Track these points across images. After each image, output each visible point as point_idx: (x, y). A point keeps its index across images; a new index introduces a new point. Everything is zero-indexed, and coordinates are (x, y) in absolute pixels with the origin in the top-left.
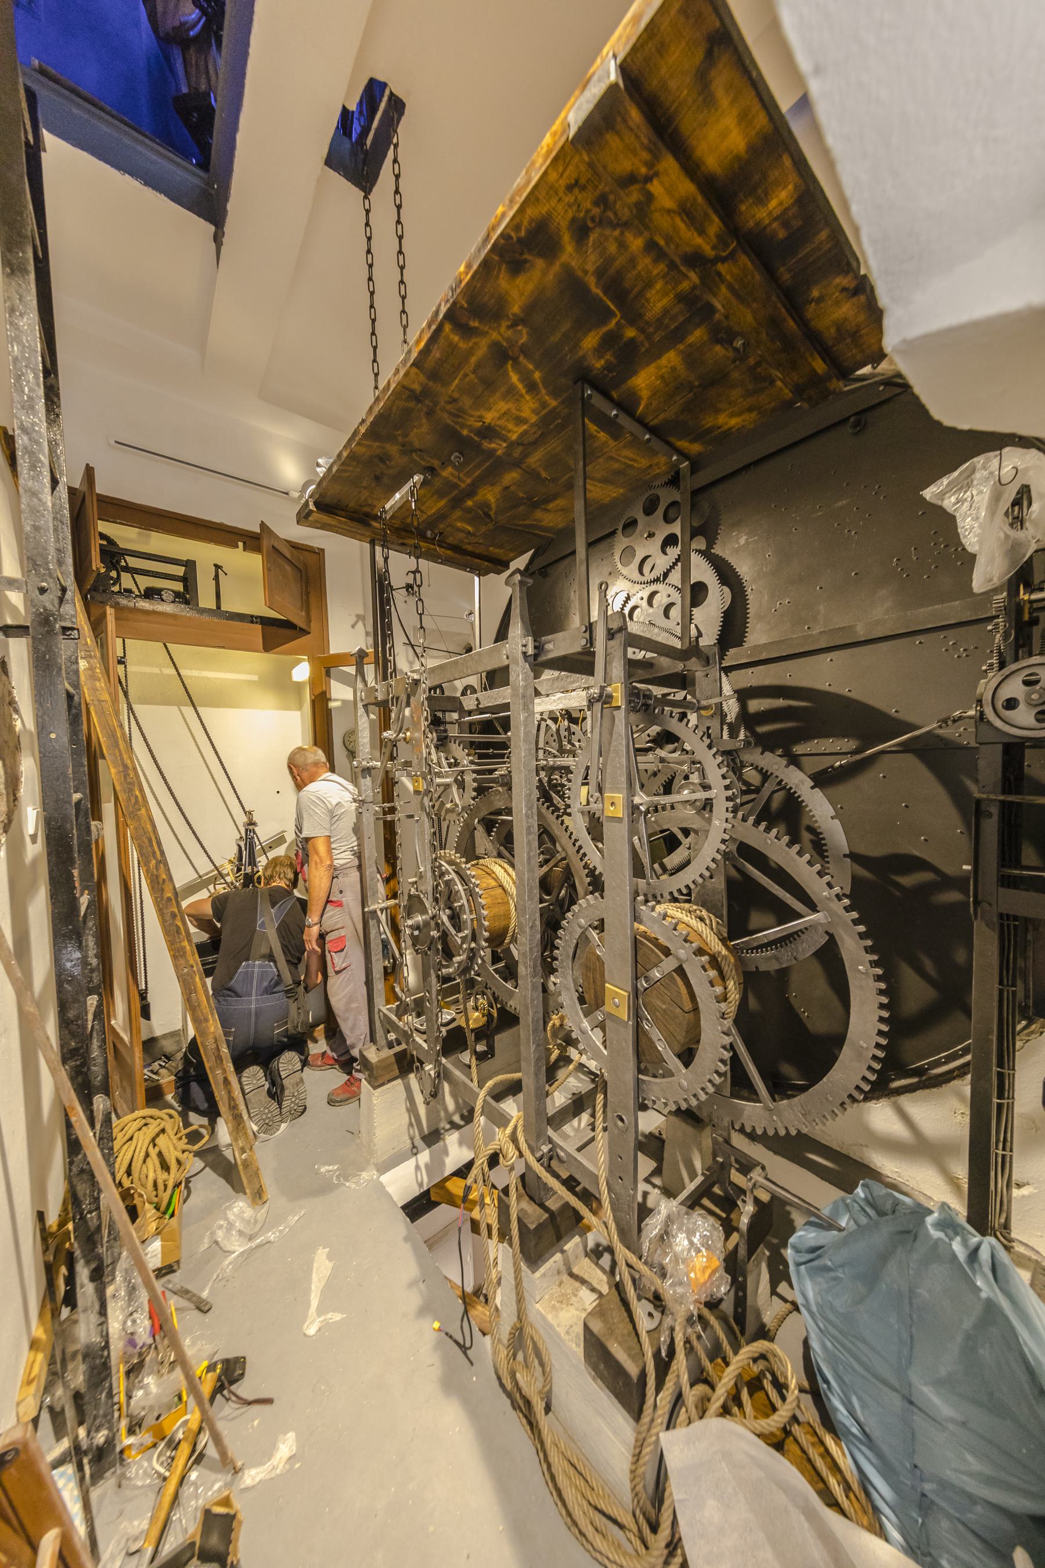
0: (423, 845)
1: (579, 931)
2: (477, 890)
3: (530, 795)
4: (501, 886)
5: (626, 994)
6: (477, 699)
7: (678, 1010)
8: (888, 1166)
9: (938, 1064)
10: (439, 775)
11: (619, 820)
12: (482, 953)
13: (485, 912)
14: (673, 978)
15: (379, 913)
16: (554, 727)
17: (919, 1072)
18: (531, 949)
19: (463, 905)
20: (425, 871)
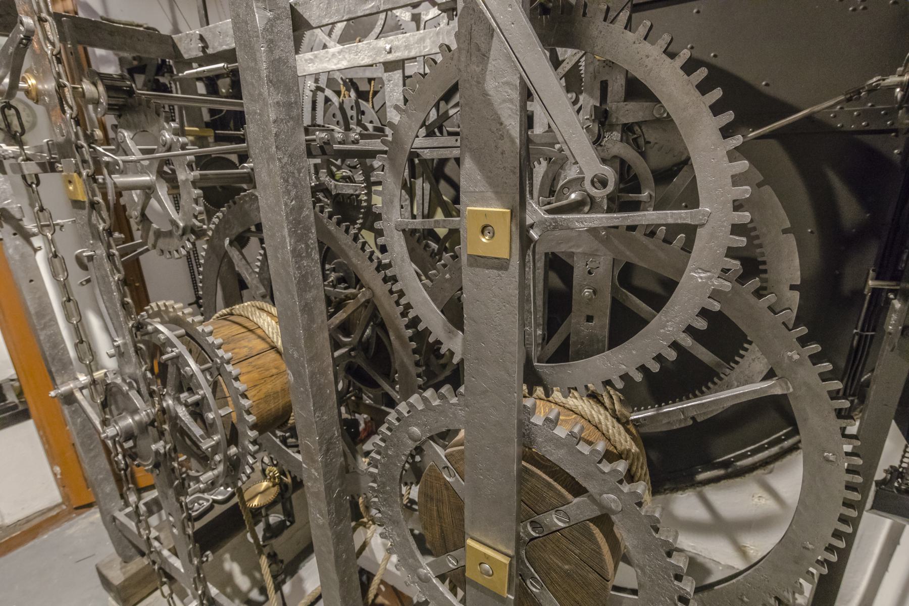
0: (111, 299)
1: (412, 445)
2: (229, 368)
3: (300, 208)
4: (273, 348)
5: (506, 560)
6: (202, 38)
7: (593, 576)
8: (688, 543)
9: (744, 456)
10: (112, 168)
11: (501, 265)
12: (251, 461)
13: (246, 403)
14: (591, 537)
15: (78, 395)
16: (335, 99)
17: (726, 464)
18: (329, 489)
19: (204, 397)
20: (125, 344)
